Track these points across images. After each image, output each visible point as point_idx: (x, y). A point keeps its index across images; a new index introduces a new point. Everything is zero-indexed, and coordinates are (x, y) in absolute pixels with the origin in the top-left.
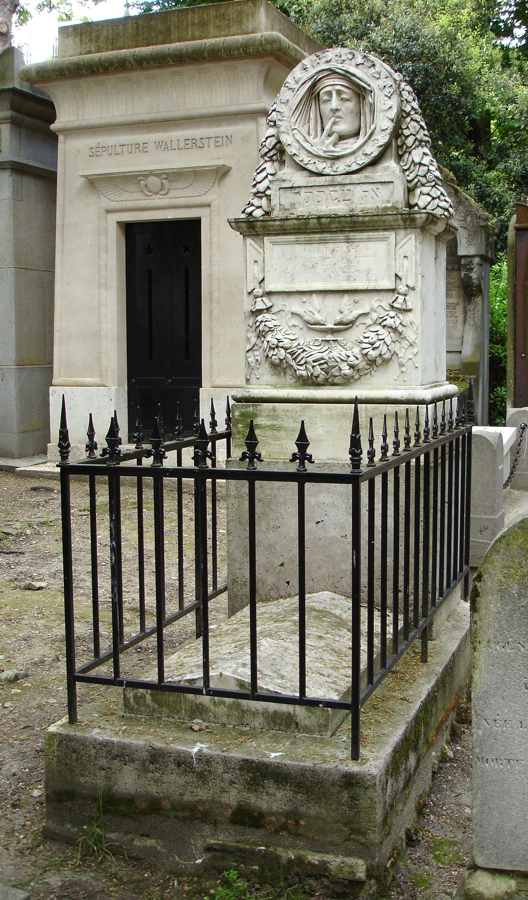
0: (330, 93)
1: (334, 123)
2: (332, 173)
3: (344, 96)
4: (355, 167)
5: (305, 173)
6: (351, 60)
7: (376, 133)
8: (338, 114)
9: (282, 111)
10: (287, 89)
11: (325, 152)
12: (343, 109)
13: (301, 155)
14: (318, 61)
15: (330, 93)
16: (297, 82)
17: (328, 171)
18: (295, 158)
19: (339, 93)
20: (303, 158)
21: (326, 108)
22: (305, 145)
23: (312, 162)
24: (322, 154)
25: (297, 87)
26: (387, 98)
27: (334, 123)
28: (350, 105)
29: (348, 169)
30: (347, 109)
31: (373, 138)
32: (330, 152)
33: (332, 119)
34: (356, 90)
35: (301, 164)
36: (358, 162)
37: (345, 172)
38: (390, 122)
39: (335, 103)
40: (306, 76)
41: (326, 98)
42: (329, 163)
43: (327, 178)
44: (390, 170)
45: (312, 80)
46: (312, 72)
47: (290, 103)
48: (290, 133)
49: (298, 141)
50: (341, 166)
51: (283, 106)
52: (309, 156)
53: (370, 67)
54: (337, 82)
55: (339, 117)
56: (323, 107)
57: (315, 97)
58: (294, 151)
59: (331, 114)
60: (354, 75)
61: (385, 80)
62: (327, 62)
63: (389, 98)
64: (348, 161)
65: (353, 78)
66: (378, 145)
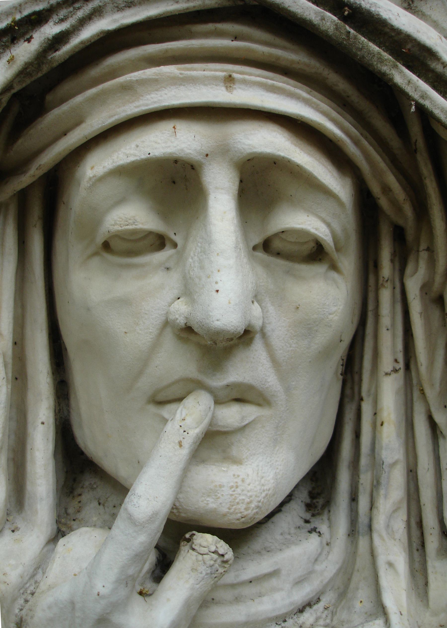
0: (175, 185)
1: (213, 442)
3: (303, 220)
8: (238, 372)
12: (278, 325)
15: (175, 185)
19: (260, 184)
21: (125, 308)
27: (213, 442)
28: (328, 296)
30: (307, 327)
33: (192, 415)
34: (388, 183)
39: (222, 274)
41: (133, 215)
55: (241, 396)
56: (90, 286)
57: (23, 197)
59: (174, 362)
65: (405, 78)
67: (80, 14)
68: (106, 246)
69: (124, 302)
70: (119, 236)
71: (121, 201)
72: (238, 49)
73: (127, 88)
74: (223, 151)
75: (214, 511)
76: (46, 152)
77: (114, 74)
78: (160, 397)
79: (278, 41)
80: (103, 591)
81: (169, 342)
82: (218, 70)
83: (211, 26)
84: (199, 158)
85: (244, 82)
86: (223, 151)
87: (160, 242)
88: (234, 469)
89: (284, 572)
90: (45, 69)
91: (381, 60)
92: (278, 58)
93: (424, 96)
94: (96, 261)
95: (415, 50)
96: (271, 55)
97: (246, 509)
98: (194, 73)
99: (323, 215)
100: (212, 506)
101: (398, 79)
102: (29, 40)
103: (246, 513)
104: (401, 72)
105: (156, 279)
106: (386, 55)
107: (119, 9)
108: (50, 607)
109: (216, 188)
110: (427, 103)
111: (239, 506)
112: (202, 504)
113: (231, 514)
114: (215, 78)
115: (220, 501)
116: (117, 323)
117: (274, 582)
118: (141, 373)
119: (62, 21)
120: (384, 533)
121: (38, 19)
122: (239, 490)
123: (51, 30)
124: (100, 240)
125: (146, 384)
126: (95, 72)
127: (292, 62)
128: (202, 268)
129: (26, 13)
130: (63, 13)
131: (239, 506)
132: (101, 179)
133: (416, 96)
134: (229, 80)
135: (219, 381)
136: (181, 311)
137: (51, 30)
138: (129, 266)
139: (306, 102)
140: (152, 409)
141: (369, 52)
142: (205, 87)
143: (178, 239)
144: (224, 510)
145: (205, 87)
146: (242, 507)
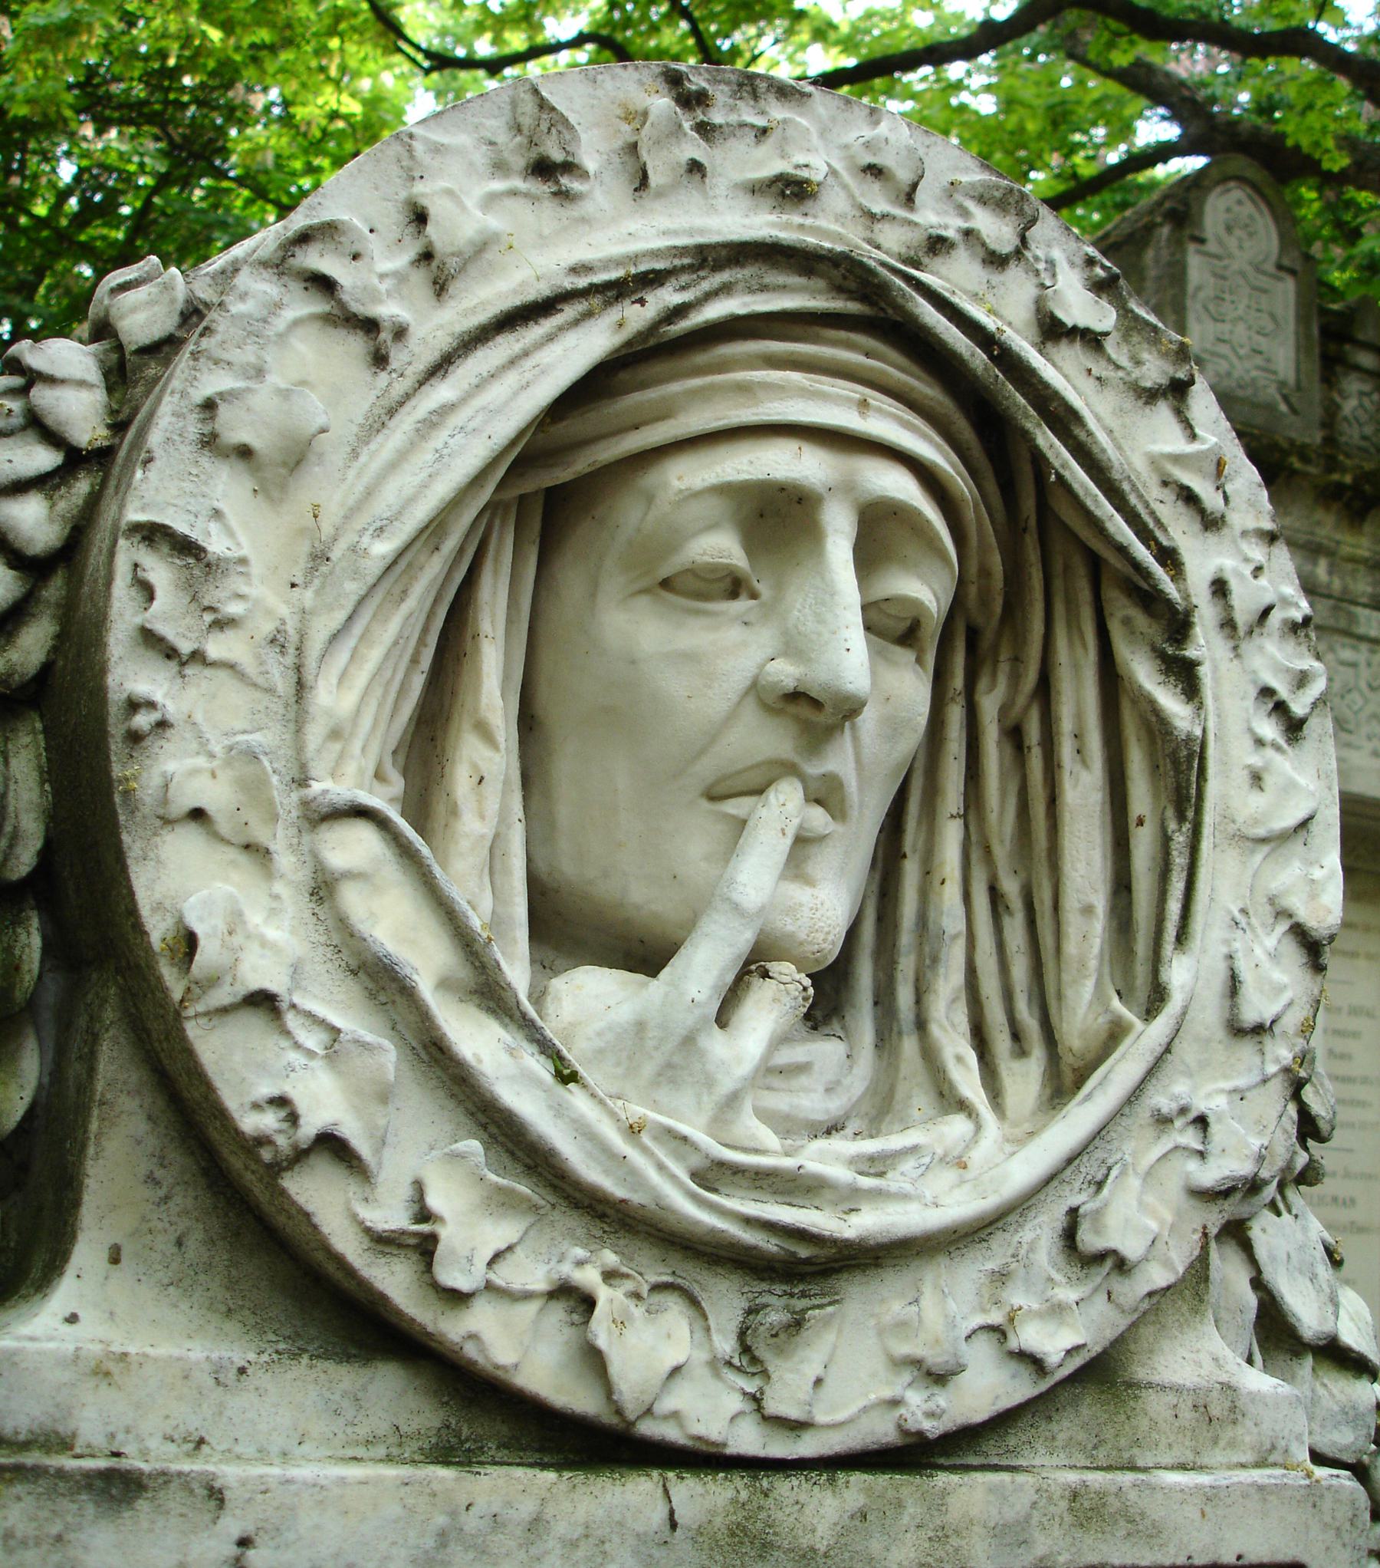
0: (778, 519)
2: (748, 1440)
4: (985, 1388)
5: (387, 1393)
6: (996, 261)
7: (1186, 1050)
9: (216, 545)
10: (304, 305)
11: (713, 1175)
13: (394, 1173)
14: (693, 148)
15: (778, 519)
16: (437, 272)
17: (710, 1411)
18: (322, 1199)
20: (403, 1187)
22: (478, 1040)
23: (531, 1273)
24: (689, 1208)
25: (432, 327)
26: (1270, 729)
29: (927, 1411)
31: (1161, 1099)
32: (764, 1180)
35: (393, 1281)
36: (1032, 1336)
37: (882, 1431)
38: (1294, 955)
40: (545, 251)
41: (721, 546)
42: (727, 1300)
43: (699, 1497)
44: (1247, 1434)
45: (637, 315)
46: (620, 231)
47: (328, 490)
48: (285, 860)
49: (381, 980)
50: (847, 1374)
51: (227, 486)
52: (502, 1202)
53: (1150, 396)
54: (887, 423)
58: (324, 1103)
59: (763, 739)
60: (1063, 419)
61: (1257, 552)
62: (792, 191)
63: (1294, 728)
64: (944, 1306)
66: (1209, 1175)
67: (706, 286)
68: (666, 584)
69: (690, 658)
70: (693, 571)
71: (711, 527)
72: (872, 369)
73: (745, 389)
74: (847, 487)
75: (791, 936)
76: (602, 445)
77: (722, 367)
78: (720, 790)
79: (914, 369)
80: (698, 997)
81: (751, 714)
82: (859, 391)
83: (843, 334)
84: (822, 490)
85: (879, 410)
86: (847, 487)
87: (735, 586)
88: (808, 890)
89: (816, 1068)
90: (652, 342)
91: (1027, 416)
92: (913, 389)
93: (1065, 465)
94: (644, 601)
95: (1061, 410)
96: (905, 384)
97: (825, 940)
98: (826, 388)
99: (936, 587)
100: (790, 928)
101: (1041, 441)
102: (642, 302)
103: (824, 946)
104: (1044, 433)
105: (734, 634)
106: (1032, 412)
107: (751, 291)
108: (599, 1034)
109: (836, 531)
110: (1067, 474)
111: (817, 935)
112: (779, 924)
113: (810, 943)
114: (849, 400)
115: (799, 923)
116: (674, 684)
117: (803, 1080)
118: (703, 752)
119: (683, 288)
120: (945, 1023)
121: (652, 279)
122: (818, 915)
123: (668, 296)
124: (664, 572)
125: (707, 769)
126: (701, 358)
127: (926, 396)
128: (820, 620)
129: (642, 268)
130: (684, 279)
131: (817, 935)
132: (696, 495)
133: (1056, 464)
134: (863, 405)
135: (814, 769)
136: (785, 673)
137: (668, 296)
138: (698, 612)
139: (937, 447)
140: (705, 804)
141: (1016, 404)
142: (835, 406)
143: (762, 588)
144: (802, 936)
145: (835, 406)
146: (821, 936)
